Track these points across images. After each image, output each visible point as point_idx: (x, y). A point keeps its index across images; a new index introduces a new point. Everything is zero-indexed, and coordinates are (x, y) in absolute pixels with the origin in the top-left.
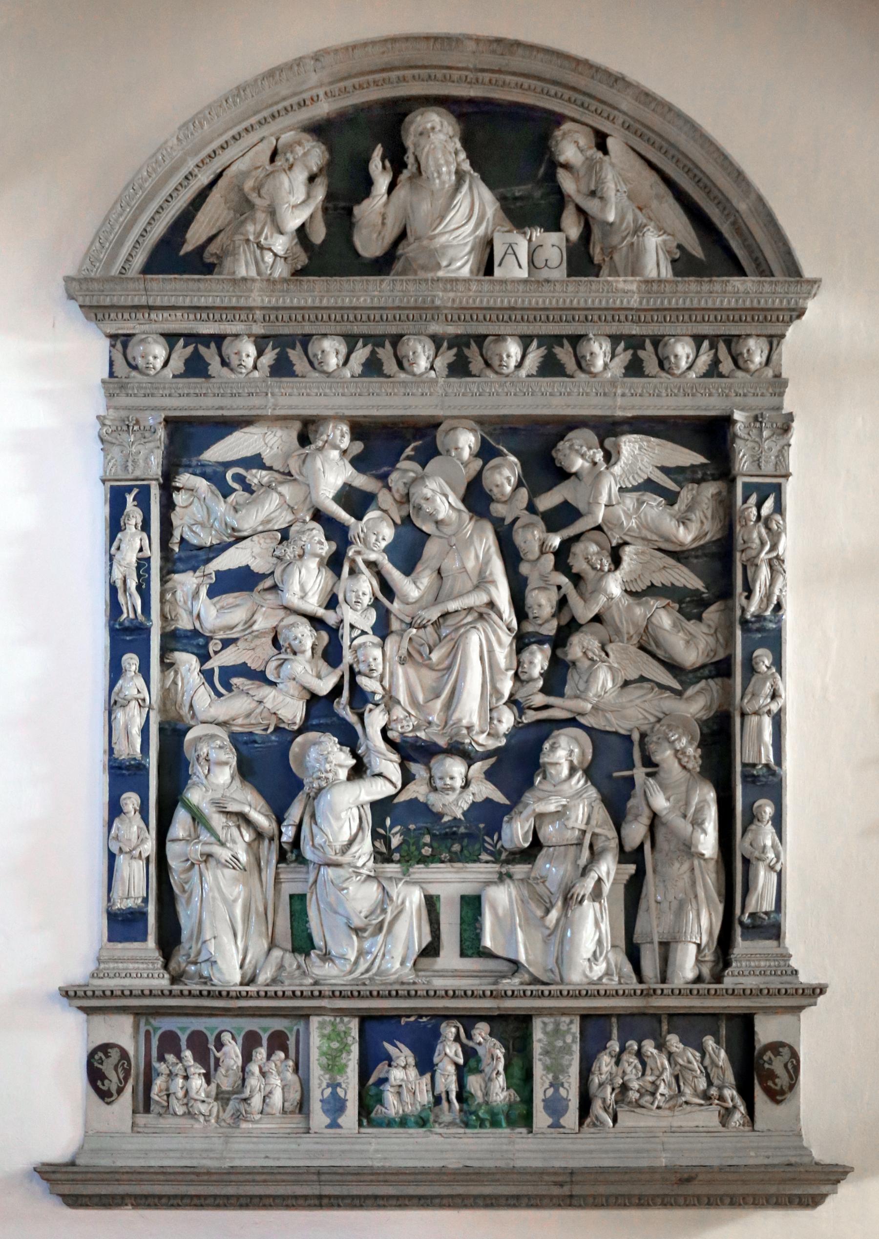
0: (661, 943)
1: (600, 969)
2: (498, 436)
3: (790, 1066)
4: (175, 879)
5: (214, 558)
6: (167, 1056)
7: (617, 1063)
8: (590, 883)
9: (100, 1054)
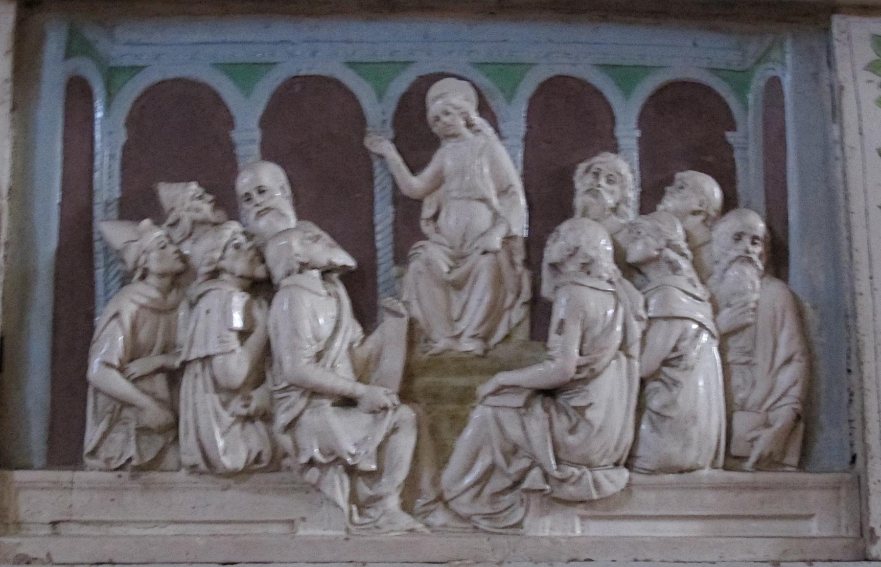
6: (167, 192)
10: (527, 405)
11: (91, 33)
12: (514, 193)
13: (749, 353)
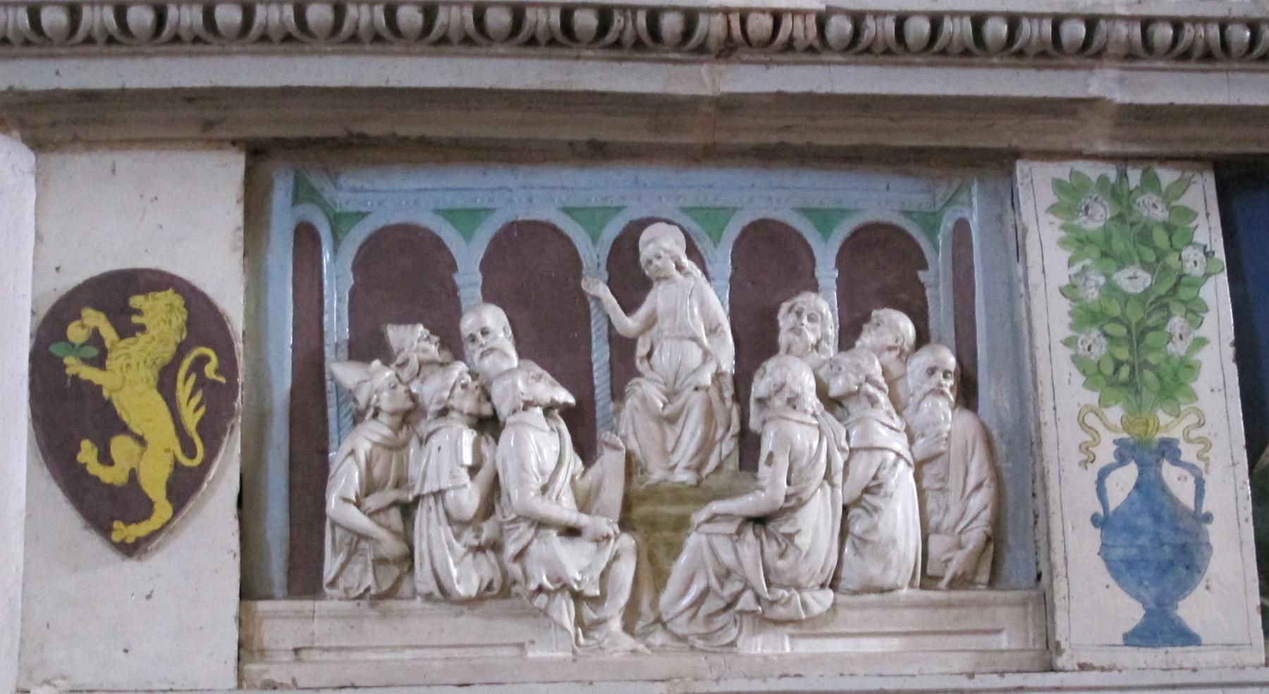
6: (396, 334)
9: (94, 319)
10: (739, 532)
11: (318, 181)
12: (723, 332)
13: (943, 480)
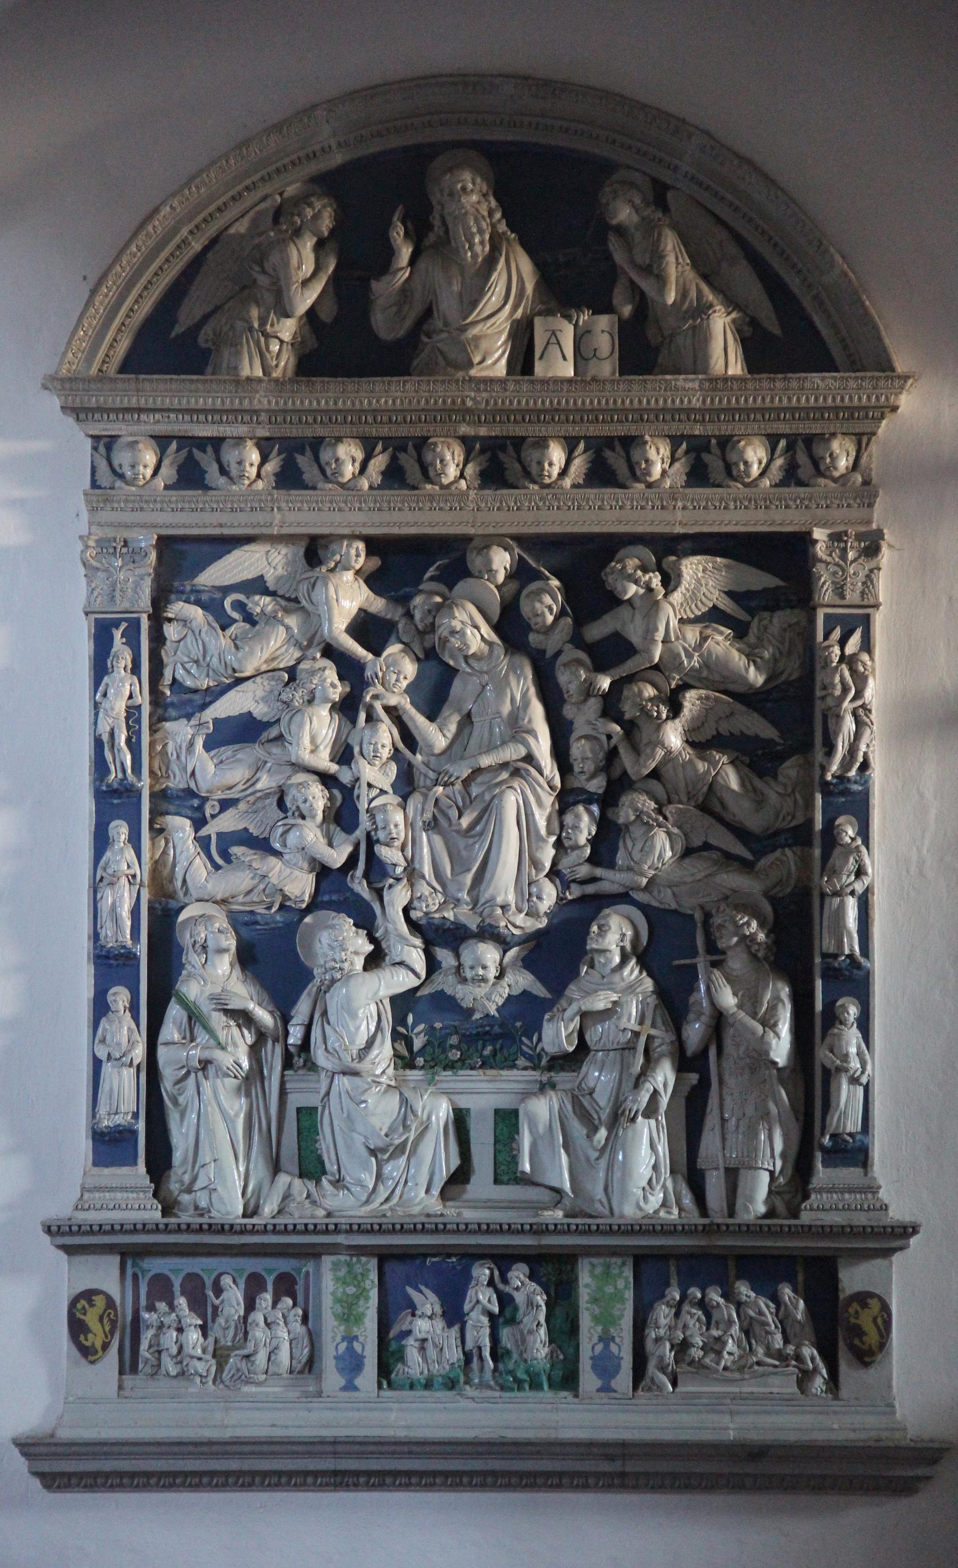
0: (727, 1170)
1: (656, 1199)
2: (540, 553)
3: (879, 1321)
4: (167, 1085)
5: (211, 703)
7: (677, 1315)
8: (644, 1097)
